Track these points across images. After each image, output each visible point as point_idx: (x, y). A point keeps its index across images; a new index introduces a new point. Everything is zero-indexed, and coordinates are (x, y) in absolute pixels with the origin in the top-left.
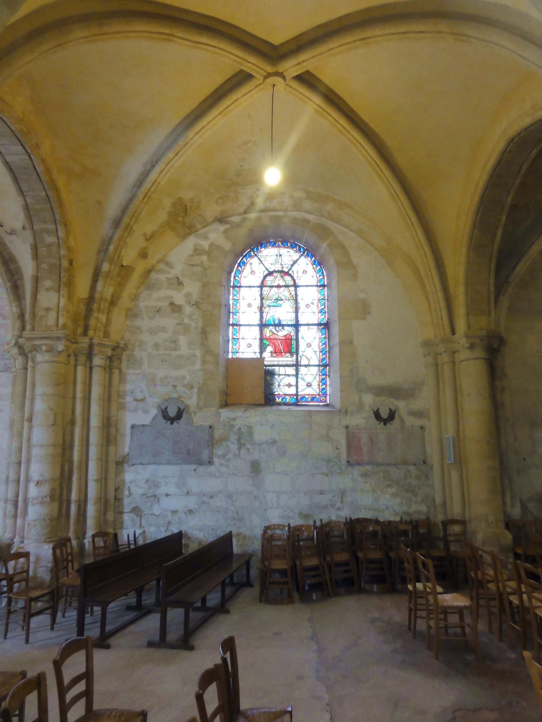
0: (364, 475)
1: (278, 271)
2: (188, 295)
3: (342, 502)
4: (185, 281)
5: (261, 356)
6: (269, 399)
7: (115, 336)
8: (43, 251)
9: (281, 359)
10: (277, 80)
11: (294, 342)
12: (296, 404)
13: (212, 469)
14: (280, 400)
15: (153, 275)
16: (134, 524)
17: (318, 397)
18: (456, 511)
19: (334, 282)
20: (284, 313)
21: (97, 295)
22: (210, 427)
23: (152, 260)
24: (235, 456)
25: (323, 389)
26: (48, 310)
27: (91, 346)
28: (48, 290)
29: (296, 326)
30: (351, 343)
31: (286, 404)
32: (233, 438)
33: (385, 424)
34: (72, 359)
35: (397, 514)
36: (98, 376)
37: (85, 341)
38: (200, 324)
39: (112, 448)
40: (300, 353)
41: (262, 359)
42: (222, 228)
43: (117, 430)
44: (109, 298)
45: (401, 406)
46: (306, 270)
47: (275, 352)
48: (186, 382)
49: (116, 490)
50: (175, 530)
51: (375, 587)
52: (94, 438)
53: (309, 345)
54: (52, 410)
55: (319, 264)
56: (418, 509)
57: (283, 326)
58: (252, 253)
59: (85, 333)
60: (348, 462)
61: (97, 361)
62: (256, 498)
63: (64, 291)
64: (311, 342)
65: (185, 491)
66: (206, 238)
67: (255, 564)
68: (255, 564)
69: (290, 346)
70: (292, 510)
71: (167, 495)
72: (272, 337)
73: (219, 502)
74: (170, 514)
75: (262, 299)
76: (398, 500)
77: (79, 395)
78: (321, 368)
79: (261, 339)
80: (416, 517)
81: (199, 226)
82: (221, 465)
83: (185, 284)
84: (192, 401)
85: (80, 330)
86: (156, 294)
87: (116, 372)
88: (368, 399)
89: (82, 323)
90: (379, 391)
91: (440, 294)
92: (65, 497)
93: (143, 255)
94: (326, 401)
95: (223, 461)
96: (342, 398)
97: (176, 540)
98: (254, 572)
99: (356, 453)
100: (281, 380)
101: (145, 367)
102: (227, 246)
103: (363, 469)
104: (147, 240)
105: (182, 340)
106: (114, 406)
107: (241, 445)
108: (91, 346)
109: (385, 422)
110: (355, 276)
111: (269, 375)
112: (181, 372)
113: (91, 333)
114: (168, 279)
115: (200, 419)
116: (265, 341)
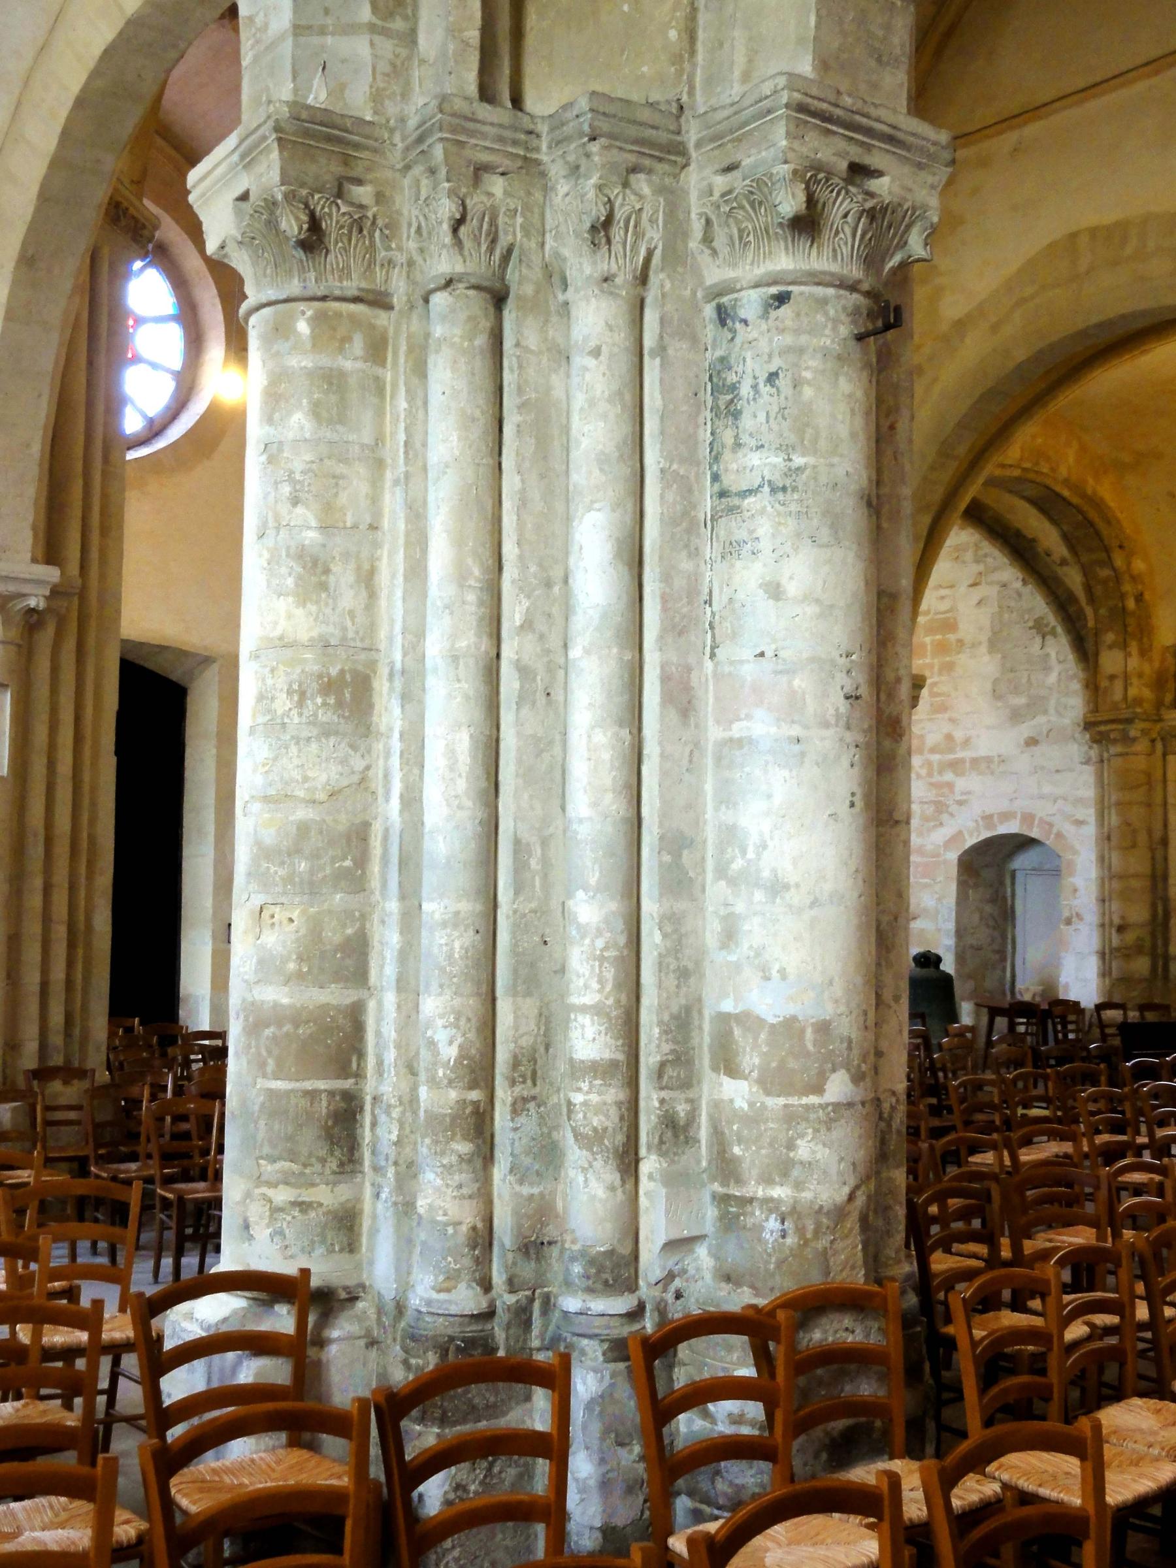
8: (1098, 590)
26: (1112, 677)
28: (1110, 647)
34: (1159, 746)
63: (1134, 648)
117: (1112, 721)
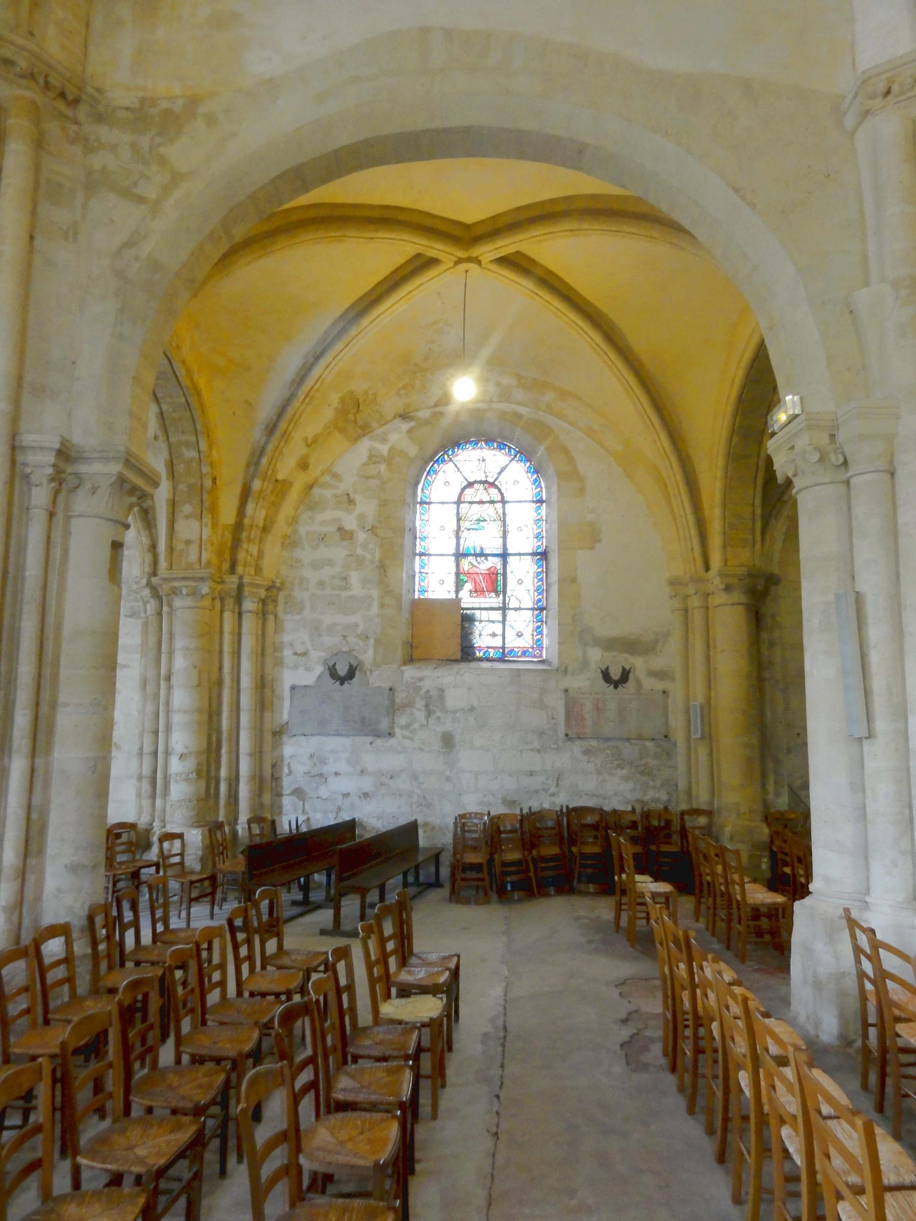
0: (586, 752)
1: (481, 482)
2: (361, 517)
3: (557, 786)
4: (358, 498)
5: (457, 596)
6: (467, 653)
7: (269, 572)
8: (180, 468)
9: (482, 600)
10: (472, 266)
11: (500, 578)
12: (502, 660)
13: (393, 741)
14: (481, 654)
15: (316, 491)
16: (296, 810)
17: (530, 650)
18: (702, 799)
19: (554, 498)
20: (487, 539)
21: (247, 521)
22: (391, 689)
23: (314, 471)
24: (422, 726)
25: (538, 640)
26: (188, 542)
27: (240, 587)
28: (187, 517)
29: (504, 556)
30: (574, 580)
31: (489, 660)
32: (420, 703)
33: (616, 687)
35: (628, 803)
36: (249, 624)
37: (232, 582)
38: (377, 557)
39: (267, 715)
40: (509, 593)
41: (457, 601)
42: (406, 426)
43: (273, 692)
44: (261, 524)
45: (638, 664)
46: (518, 480)
47: (476, 591)
48: (359, 632)
49: (273, 766)
50: (347, 818)
51: (591, 888)
52: (246, 701)
53: (520, 582)
54: (195, 667)
55: (536, 471)
56: (655, 796)
57: (486, 556)
58: (446, 457)
59: (232, 569)
60: (567, 735)
61: (249, 605)
62: (448, 779)
63: (207, 518)
64: (523, 577)
65: (358, 769)
66: (384, 440)
67: (446, 860)
68: (446, 860)
69: (495, 583)
70: (494, 795)
71: (336, 774)
72: (472, 571)
73: (402, 783)
74: (340, 798)
75: (459, 519)
76: (630, 785)
77: (227, 648)
78: (536, 612)
79: (458, 574)
80: (652, 806)
81: (375, 425)
82: (404, 737)
83: (357, 502)
84: (367, 656)
85: (226, 566)
86: (320, 517)
87: (271, 618)
88: (596, 655)
89: (227, 556)
90: (609, 644)
91: (691, 518)
92: (213, 773)
93: (304, 465)
94: (541, 656)
95: (406, 733)
96: (560, 653)
97: (350, 826)
98: (445, 872)
99: (575, 725)
100: (483, 628)
101: (307, 612)
102: (413, 451)
103: (585, 744)
104: (308, 445)
105: (355, 577)
106: (269, 661)
107: (429, 713)
108: (240, 587)
109: (616, 684)
110: (582, 491)
111: (467, 620)
112: (353, 619)
113: (240, 570)
114: (336, 496)
115: (379, 679)
116: (462, 577)
117: (184, 579)
